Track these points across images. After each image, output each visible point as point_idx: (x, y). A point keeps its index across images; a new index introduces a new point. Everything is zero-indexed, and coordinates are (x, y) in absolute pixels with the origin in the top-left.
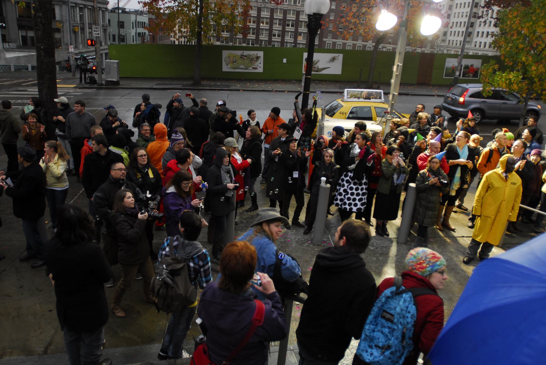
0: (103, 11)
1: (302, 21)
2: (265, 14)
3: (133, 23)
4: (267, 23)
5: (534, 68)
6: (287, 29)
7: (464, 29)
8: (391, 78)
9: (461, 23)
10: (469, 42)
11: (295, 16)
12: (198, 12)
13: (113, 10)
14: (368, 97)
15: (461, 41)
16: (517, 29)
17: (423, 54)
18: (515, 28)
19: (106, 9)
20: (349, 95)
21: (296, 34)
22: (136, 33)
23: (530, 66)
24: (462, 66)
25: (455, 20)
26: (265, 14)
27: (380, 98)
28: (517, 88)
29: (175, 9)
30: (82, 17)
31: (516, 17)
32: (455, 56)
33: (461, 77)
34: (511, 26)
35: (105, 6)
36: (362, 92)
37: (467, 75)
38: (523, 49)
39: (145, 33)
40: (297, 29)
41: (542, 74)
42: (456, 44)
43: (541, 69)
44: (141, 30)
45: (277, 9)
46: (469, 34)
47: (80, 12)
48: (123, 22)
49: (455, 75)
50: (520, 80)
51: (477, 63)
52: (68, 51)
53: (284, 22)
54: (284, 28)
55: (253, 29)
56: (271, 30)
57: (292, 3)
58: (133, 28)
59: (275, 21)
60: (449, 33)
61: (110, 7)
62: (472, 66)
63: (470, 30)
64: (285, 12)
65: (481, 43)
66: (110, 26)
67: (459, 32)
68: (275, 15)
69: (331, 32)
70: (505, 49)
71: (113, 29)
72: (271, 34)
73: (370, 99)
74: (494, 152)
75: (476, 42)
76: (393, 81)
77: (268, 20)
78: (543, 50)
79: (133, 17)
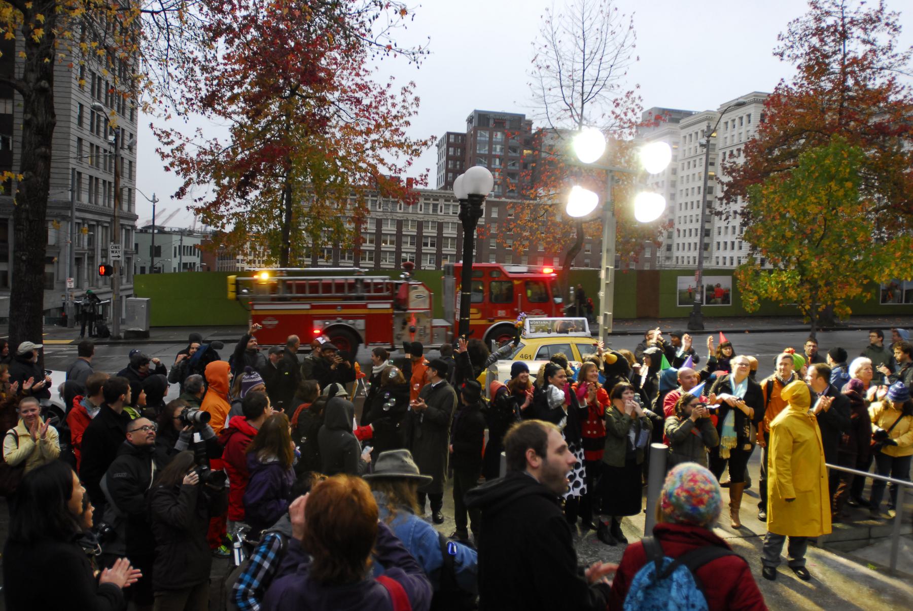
0: (127, 231)
1: (447, 238)
2: (389, 228)
4: (392, 243)
5: (814, 263)
6: (425, 250)
7: (697, 240)
8: (598, 289)
9: (692, 203)
11: (435, 231)
12: (284, 220)
13: (145, 230)
14: (564, 330)
15: (696, 244)
16: (777, 210)
17: (641, 273)
18: (774, 209)
19: (134, 227)
20: (533, 327)
21: (439, 257)
22: (179, 264)
23: (807, 261)
24: (702, 287)
25: (684, 187)
26: (389, 228)
27: (584, 330)
28: (795, 295)
29: (246, 216)
30: (91, 240)
31: (775, 192)
32: (689, 273)
33: (704, 305)
34: (768, 206)
35: (131, 223)
36: (554, 321)
37: (713, 301)
38: (792, 238)
41: (828, 273)
42: (689, 262)
43: (826, 265)
44: (187, 259)
46: (705, 247)
47: (89, 231)
48: (159, 247)
49: (694, 299)
51: (725, 282)
52: (67, 288)
53: (419, 241)
56: (398, 252)
57: (431, 212)
58: (175, 256)
59: (404, 239)
60: (674, 247)
61: (140, 224)
62: (718, 286)
63: (706, 240)
64: (420, 225)
65: (725, 258)
66: (137, 253)
67: (690, 244)
68: (404, 229)
70: (767, 239)
71: (143, 259)
73: (567, 332)
75: (717, 257)
76: (602, 294)
77: (394, 238)
78: (822, 238)
79: (176, 239)
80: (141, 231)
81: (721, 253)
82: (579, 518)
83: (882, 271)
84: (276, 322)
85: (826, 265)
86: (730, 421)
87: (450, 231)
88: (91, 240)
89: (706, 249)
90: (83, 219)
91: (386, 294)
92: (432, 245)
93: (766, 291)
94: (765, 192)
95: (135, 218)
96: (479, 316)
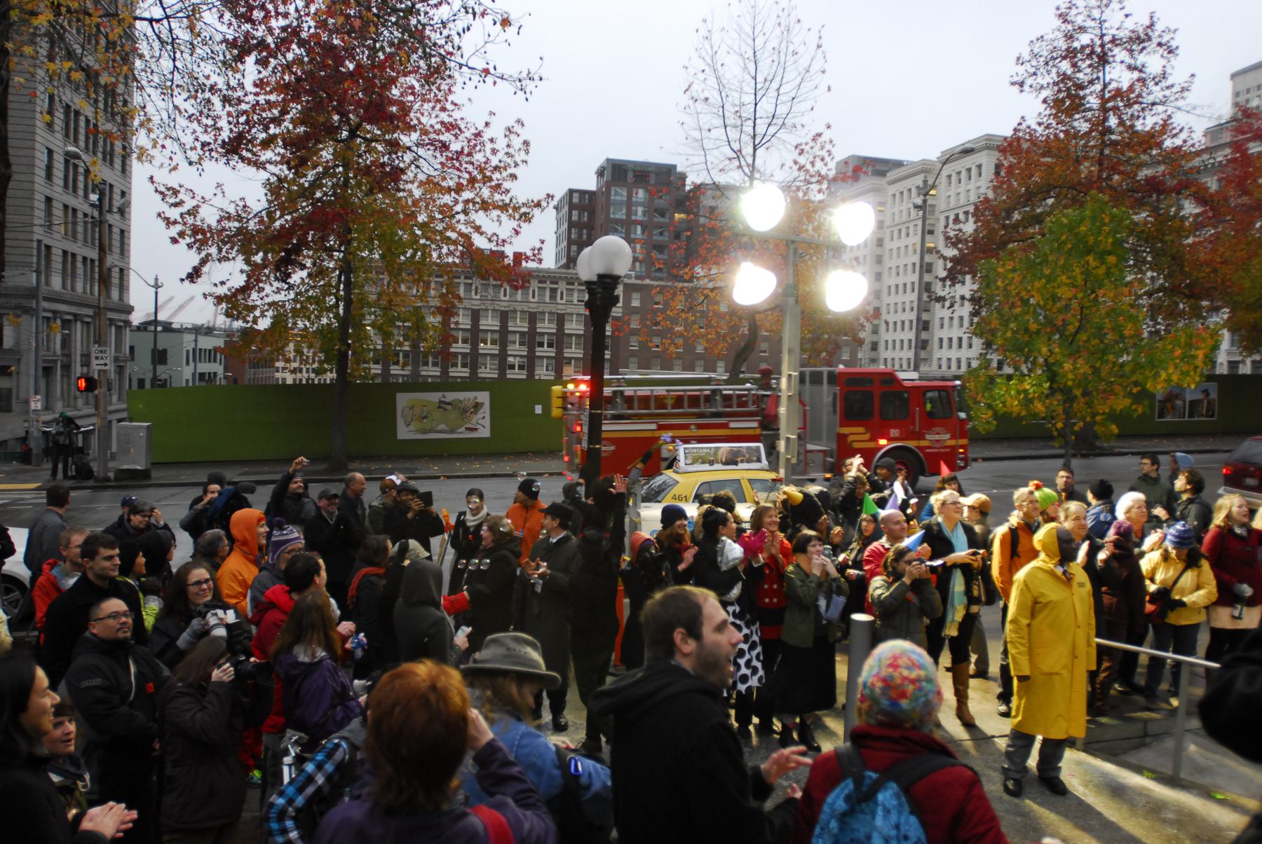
0: (119, 328)
1: (571, 335)
2: (489, 323)
3: (188, 352)
5: (1067, 366)
6: (539, 352)
7: (912, 335)
9: (905, 285)
10: (925, 360)
11: (554, 326)
12: (341, 312)
13: (143, 327)
14: (732, 460)
16: (1018, 294)
18: (1014, 293)
22: (194, 374)
23: (1060, 364)
25: (893, 264)
26: (489, 323)
27: (759, 460)
29: (288, 307)
30: (66, 342)
34: (1005, 289)
35: (123, 317)
36: (717, 449)
38: (1038, 332)
39: (215, 374)
40: (560, 352)
41: (1086, 378)
43: (1083, 367)
44: (205, 367)
45: (515, 311)
46: (923, 345)
47: (63, 327)
48: (165, 351)
50: (1046, 392)
53: (531, 339)
54: (531, 351)
55: (464, 355)
56: (502, 356)
57: (547, 300)
58: (188, 363)
59: (511, 338)
60: (882, 346)
61: (136, 318)
63: (924, 335)
64: (533, 318)
65: (949, 360)
66: (133, 359)
67: (902, 341)
68: (510, 324)
69: (633, 354)
71: (141, 367)
72: (503, 366)
73: (736, 463)
74: (1021, 533)
76: (782, 410)
77: (497, 336)
78: (1077, 332)
79: (188, 339)
80: (139, 328)
81: (944, 354)
82: (756, 720)
83: (1157, 375)
84: (612, 448)
85: (1083, 367)
86: (958, 584)
87: (574, 325)
88: (66, 342)
89: (924, 348)
90: (54, 312)
91: (752, 408)
92: (550, 345)
93: (1004, 403)
94: (1000, 270)
95: (130, 310)
96: (867, 436)
